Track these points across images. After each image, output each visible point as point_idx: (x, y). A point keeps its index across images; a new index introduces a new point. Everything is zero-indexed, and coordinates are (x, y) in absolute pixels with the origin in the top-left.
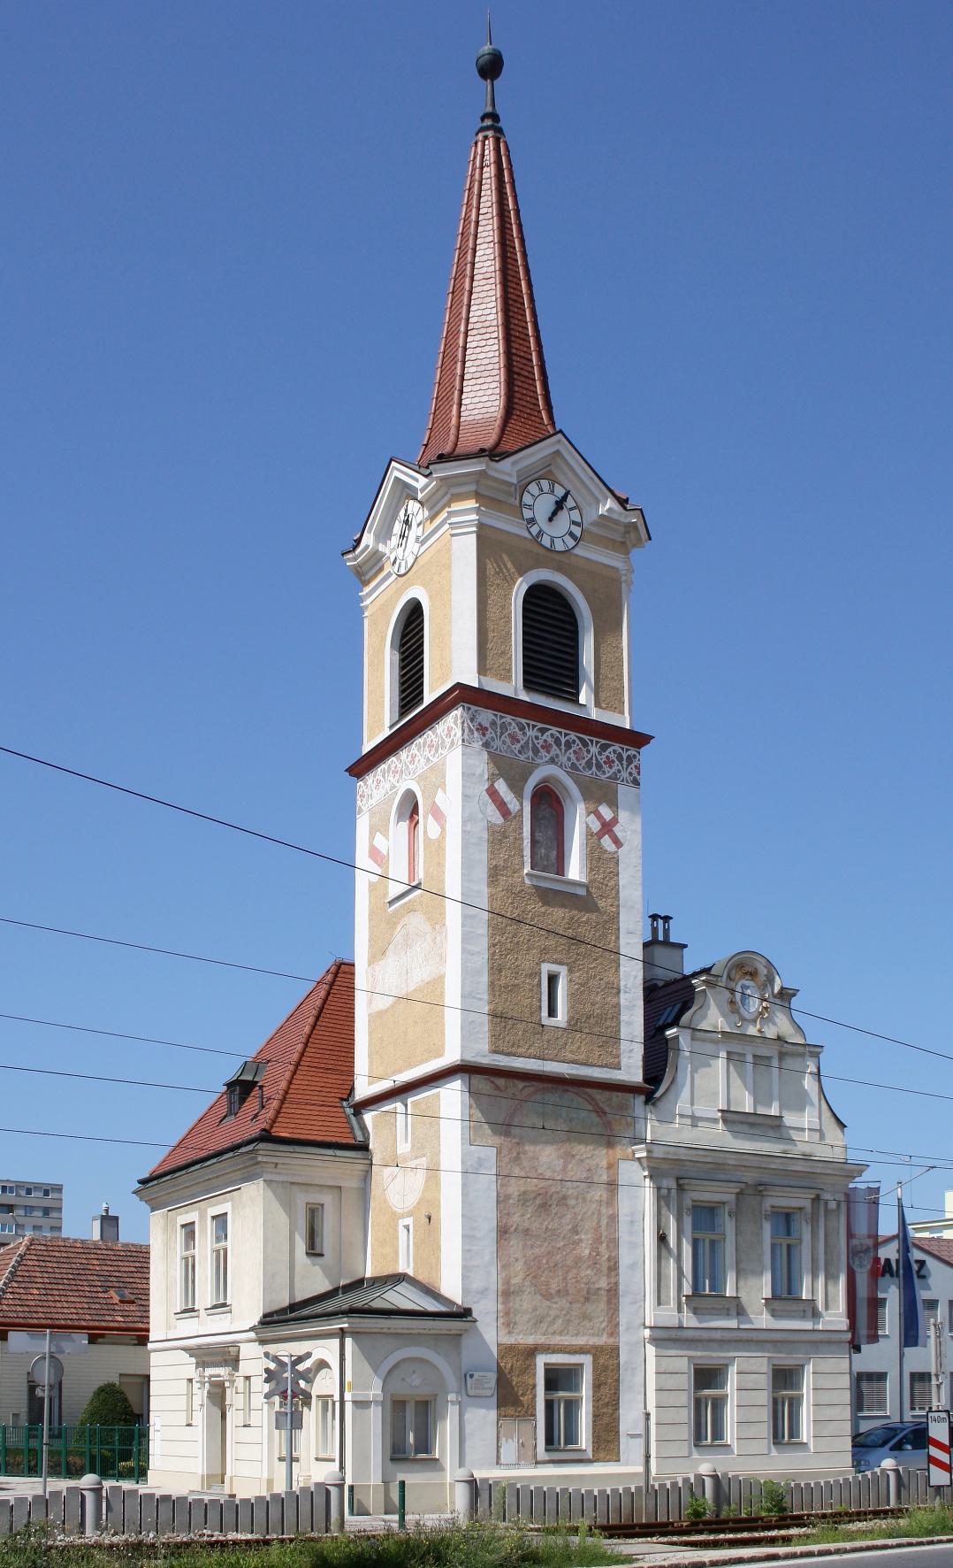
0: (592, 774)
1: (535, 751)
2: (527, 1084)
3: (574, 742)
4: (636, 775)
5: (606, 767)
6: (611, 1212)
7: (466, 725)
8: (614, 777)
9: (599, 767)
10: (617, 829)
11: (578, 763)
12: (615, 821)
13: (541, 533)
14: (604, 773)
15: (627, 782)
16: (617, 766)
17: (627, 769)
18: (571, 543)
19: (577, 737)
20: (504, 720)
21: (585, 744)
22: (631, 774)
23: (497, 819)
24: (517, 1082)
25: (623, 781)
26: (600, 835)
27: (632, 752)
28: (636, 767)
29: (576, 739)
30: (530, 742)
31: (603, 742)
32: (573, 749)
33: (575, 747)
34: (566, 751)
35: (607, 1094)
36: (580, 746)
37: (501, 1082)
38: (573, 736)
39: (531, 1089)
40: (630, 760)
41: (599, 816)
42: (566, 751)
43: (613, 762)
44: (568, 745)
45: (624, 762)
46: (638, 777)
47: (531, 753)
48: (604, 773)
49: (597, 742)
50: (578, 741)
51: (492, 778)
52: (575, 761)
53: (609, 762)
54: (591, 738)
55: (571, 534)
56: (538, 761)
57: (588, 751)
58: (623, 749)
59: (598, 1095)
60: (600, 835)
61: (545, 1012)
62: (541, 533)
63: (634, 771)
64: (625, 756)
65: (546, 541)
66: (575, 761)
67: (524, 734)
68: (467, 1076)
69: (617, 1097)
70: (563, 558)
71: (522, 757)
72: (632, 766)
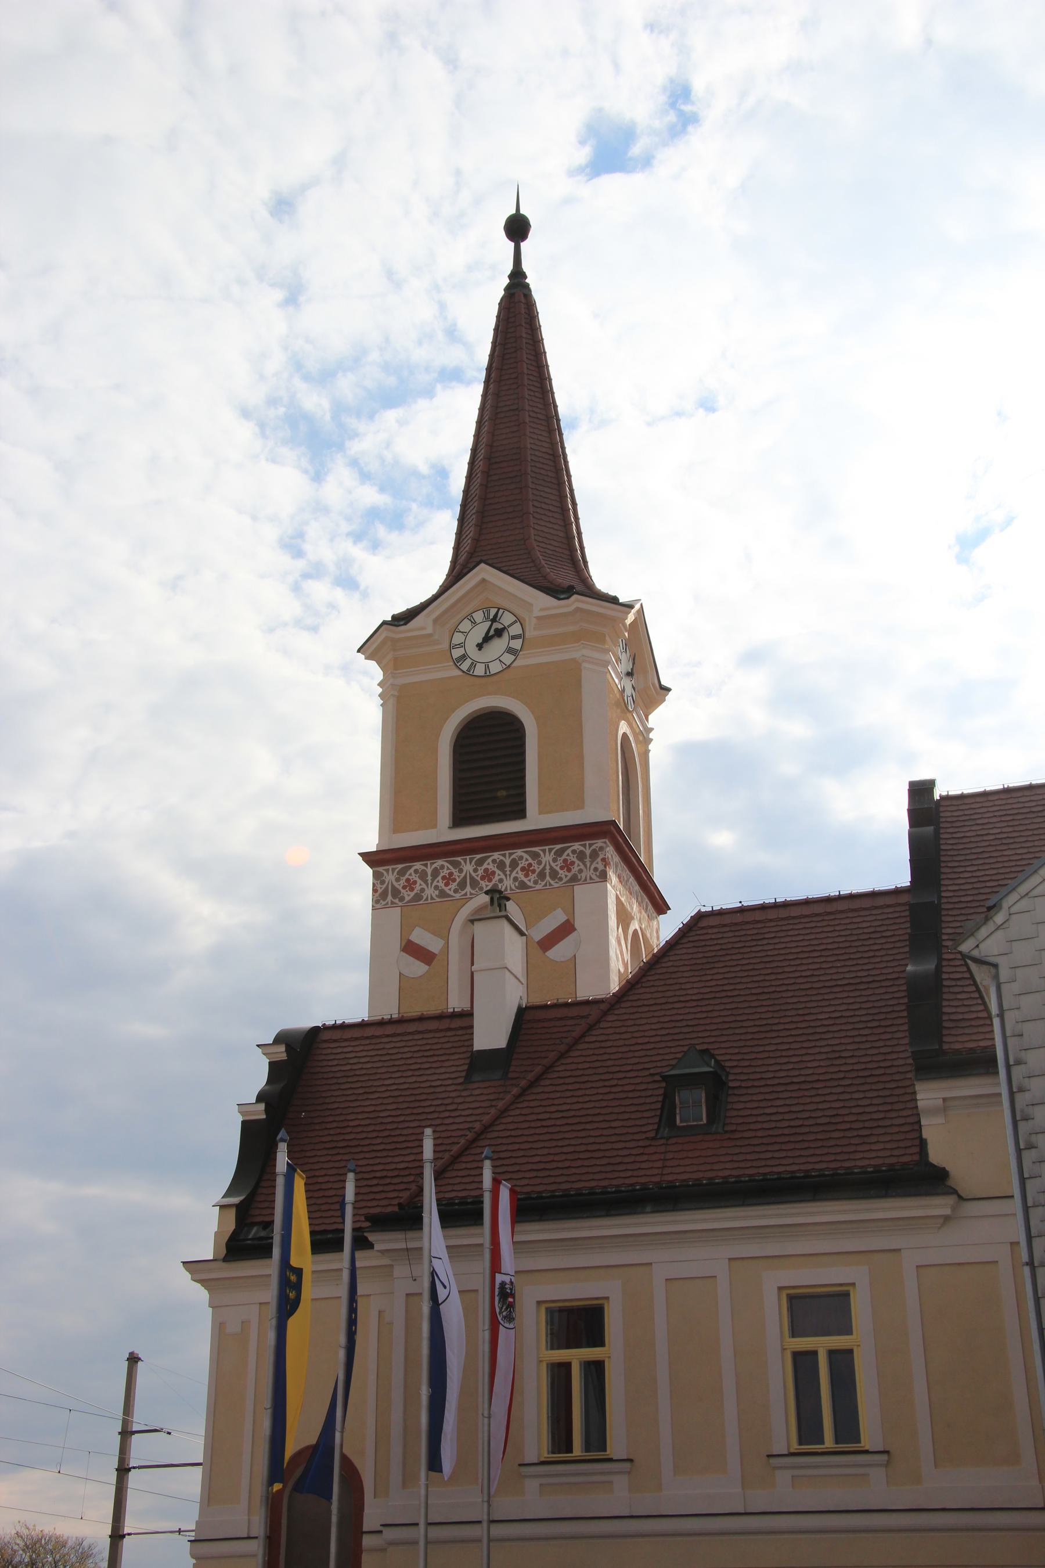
9: (554, 874)
16: (578, 866)
44: (514, 864)
54: (544, 848)
55: (510, 651)
62: (473, 665)
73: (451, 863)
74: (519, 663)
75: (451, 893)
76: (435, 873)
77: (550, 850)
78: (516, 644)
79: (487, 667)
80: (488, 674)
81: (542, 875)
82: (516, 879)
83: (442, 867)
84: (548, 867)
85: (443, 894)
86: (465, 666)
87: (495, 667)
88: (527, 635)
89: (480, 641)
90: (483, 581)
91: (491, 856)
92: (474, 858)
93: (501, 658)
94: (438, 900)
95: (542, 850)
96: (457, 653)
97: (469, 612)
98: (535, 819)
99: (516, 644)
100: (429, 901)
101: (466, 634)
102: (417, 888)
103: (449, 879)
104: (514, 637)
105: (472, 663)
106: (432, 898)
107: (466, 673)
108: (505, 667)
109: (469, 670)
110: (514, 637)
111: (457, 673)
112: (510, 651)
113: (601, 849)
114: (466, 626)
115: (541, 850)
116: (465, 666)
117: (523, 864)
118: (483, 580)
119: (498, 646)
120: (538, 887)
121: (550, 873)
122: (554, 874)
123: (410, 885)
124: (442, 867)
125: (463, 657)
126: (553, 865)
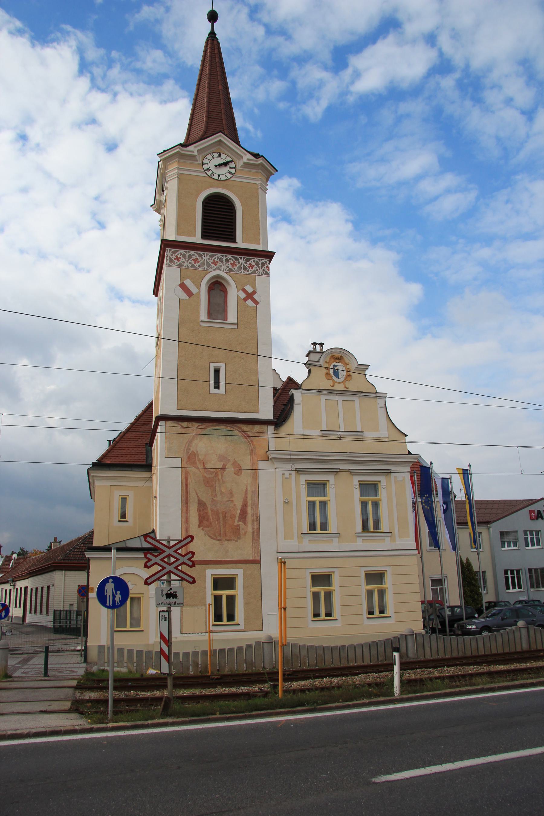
0: (241, 272)
1: (208, 265)
2: (200, 424)
3: (230, 259)
4: (267, 271)
5: (249, 269)
6: (254, 490)
7: (168, 257)
8: (254, 272)
9: (245, 269)
10: (255, 296)
11: (233, 268)
12: (254, 292)
13: (213, 174)
14: (248, 271)
15: (262, 274)
17: (261, 269)
18: (229, 176)
19: (232, 257)
20: (190, 253)
21: (236, 259)
22: (264, 270)
23: (184, 296)
24: (194, 423)
25: (259, 274)
26: (245, 300)
27: (265, 260)
28: (267, 267)
29: (231, 257)
30: (205, 261)
31: (247, 257)
32: (230, 262)
33: (231, 261)
34: (226, 264)
35: (250, 426)
36: (234, 260)
37: (185, 424)
38: (230, 256)
39: (203, 427)
40: (263, 264)
41: (244, 291)
42: (226, 264)
43: (254, 266)
44: (227, 261)
45: (260, 266)
46: (268, 271)
47: (205, 266)
48: (248, 271)
49: (244, 258)
50: (232, 259)
51: (182, 278)
52: (231, 267)
53: (251, 266)
54: (241, 256)
55: (230, 173)
56: (210, 270)
57: (239, 263)
58: (259, 260)
59: (245, 427)
60: (245, 300)
61: (212, 385)
62: (213, 174)
63: (266, 270)
64: (260, 263)
65: (216, 177)
66: (231, 267)
67: (202, 258)
68: (164, 421)
69: (257, 428)
70: (226, 182)
71: (200, 269)
72: (265, 266)
73: (197, 253)
74: (232, 179)
75: (197, 267)
76: (190, 257)
77: (244, 258)
78: (233, 171)
79: (219, 176)
80: (220, 179)
81: (240, 268)
82: (228, 267)
83: (194, 255)
84: (242, 265)
85: (193, 266)
86: (209, 173)
87: (223, 178)
88: (237, 168)
89: (217, 164)
90: (220, 141)
91: (253, 259)
92: (209, 254)
93: (225, 175)
94: (191, 268)
95: (203, 254)
96: (205, 167)
97: (212, 152)
98: (240, 243)
99: (233, 171)
100: (187, 268)
101: (210, 160)
102: (181, 261)
103: (196, 261)
104: (231, 168)
105: (212, 173)
106: (188, 267)
107: (210, 177)
108: (227, 178)
109: (211, 175)
110: (231, 168)
111: (205, 175)
112: (230, 173)
113: (266, 262)
114: (210, 157)
115: (203, 254)
116: (209, 173)
117: (194, 257)
118: (220, 141)
119: (225, 170)
120: (237, 272)
121: (243, 268)
122: (245, 269)
123: (178, 259)
124: (194, 255)
125: (208, 170)
126: (245, 265)
